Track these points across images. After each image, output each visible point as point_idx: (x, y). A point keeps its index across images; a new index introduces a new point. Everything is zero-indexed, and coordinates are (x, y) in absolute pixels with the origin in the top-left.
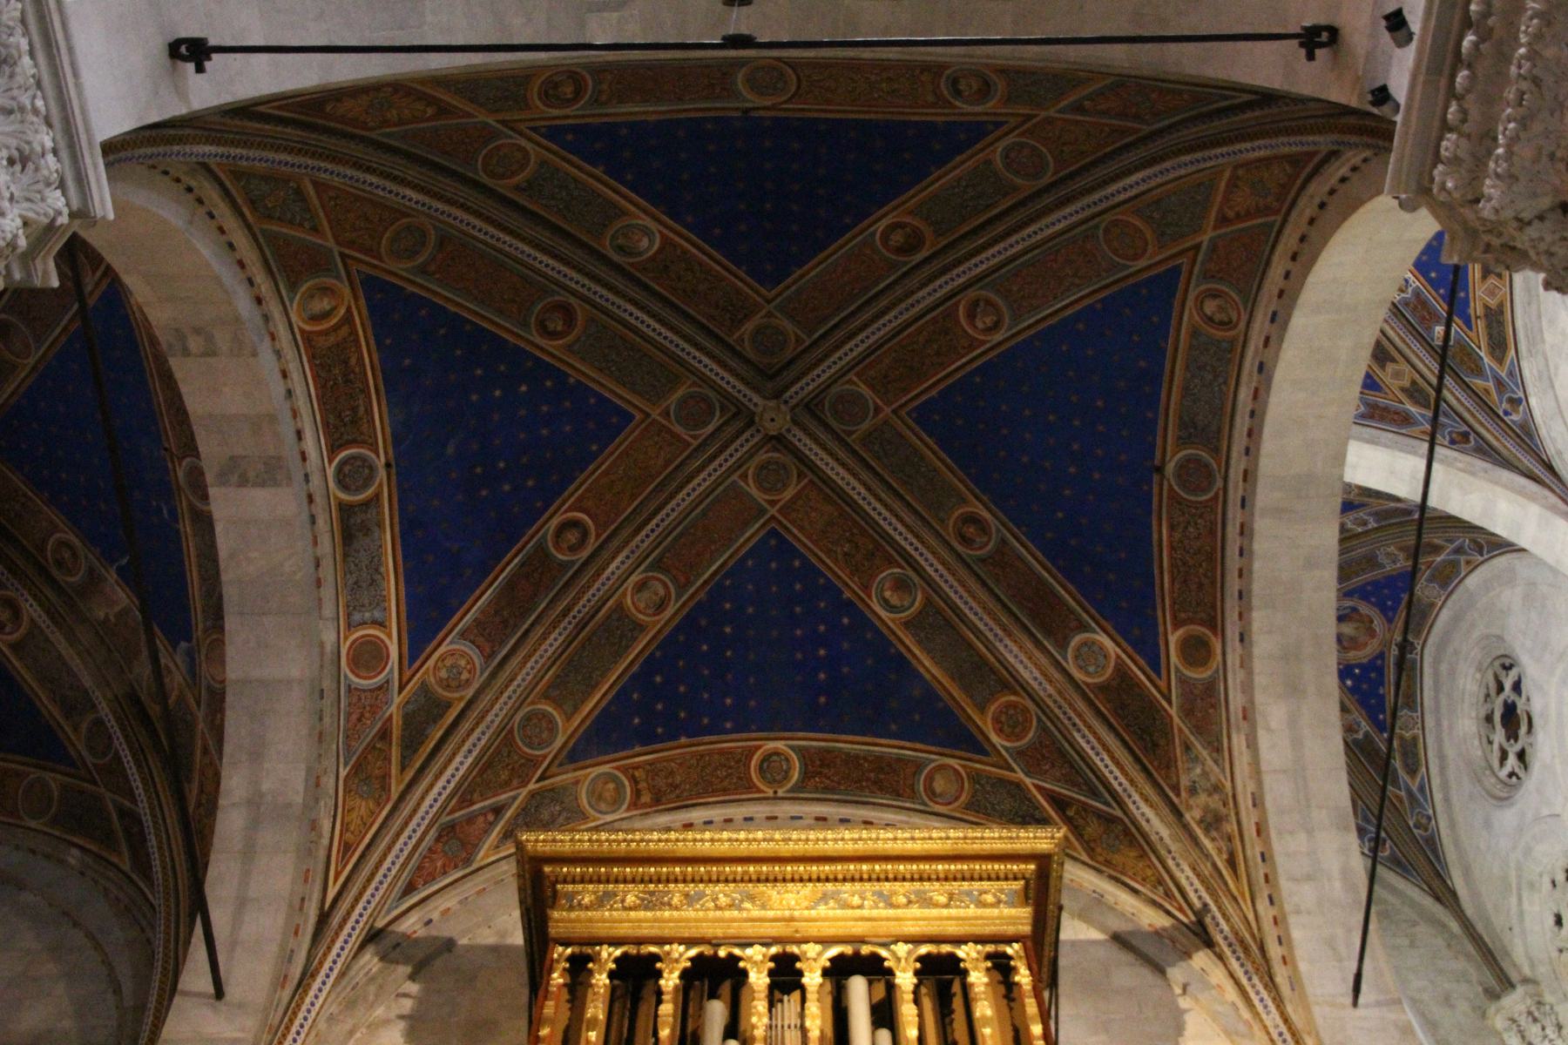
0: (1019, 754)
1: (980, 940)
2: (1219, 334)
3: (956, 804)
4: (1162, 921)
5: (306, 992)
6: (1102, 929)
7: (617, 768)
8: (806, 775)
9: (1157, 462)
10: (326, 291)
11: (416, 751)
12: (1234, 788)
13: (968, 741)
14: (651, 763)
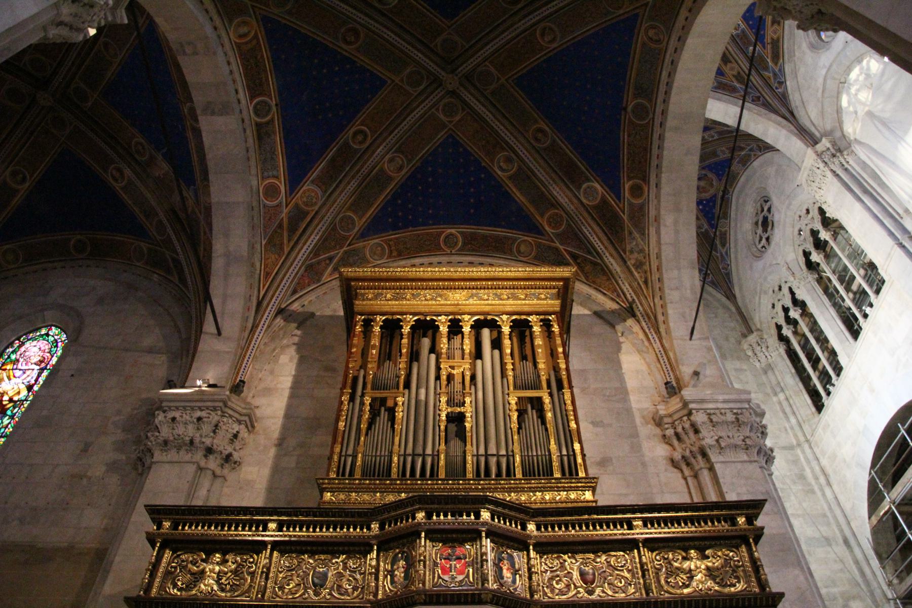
0: (558, 235)
1: (537, 314)
2: (653, 46)
4: (615, 306)
5: (254, 334)
6: (590, 309)
7: (382, 241)
8: (464, 244)
9: (624, 105)
10: (245, 23)
11: (294, 233)
12: (649, 251)
13: (534, 229)
14: (396, 239)
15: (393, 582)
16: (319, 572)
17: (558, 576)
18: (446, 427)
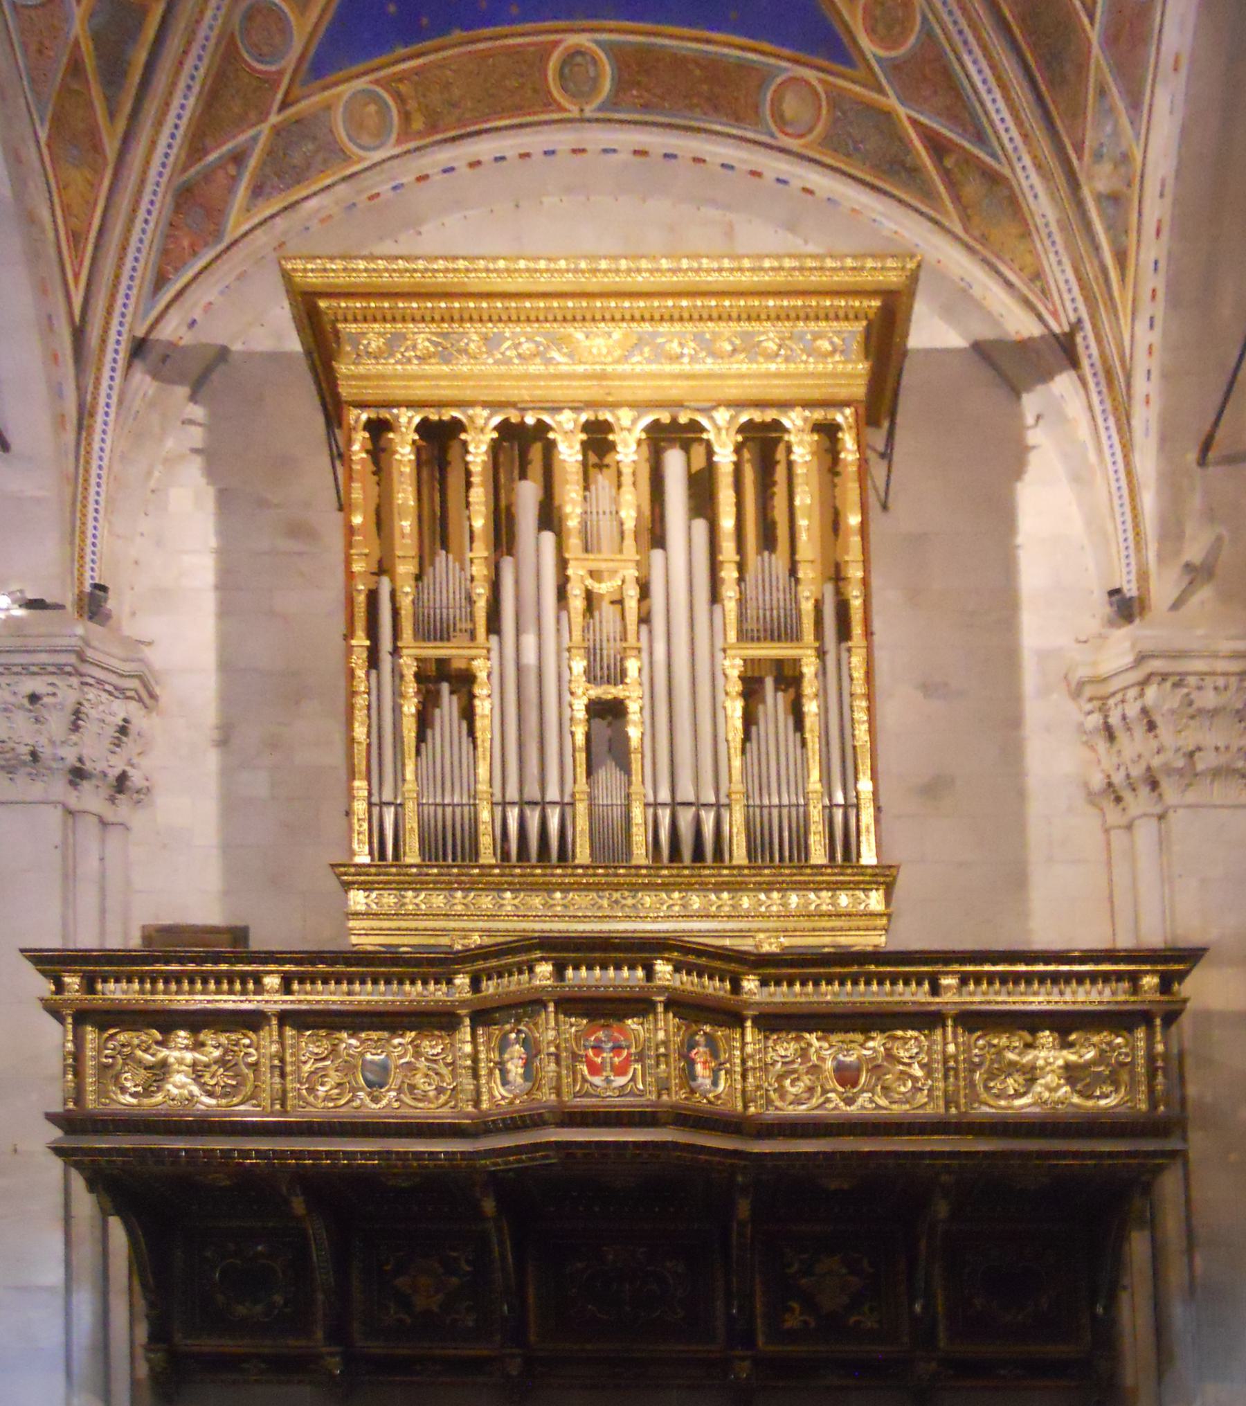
3: (810, 138)
8: (621, 85)
15: (505, 1082)
16: (372, 1062)
17: (794, 1071)
18: (588, 736)
